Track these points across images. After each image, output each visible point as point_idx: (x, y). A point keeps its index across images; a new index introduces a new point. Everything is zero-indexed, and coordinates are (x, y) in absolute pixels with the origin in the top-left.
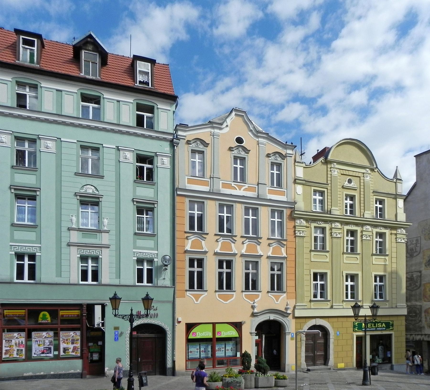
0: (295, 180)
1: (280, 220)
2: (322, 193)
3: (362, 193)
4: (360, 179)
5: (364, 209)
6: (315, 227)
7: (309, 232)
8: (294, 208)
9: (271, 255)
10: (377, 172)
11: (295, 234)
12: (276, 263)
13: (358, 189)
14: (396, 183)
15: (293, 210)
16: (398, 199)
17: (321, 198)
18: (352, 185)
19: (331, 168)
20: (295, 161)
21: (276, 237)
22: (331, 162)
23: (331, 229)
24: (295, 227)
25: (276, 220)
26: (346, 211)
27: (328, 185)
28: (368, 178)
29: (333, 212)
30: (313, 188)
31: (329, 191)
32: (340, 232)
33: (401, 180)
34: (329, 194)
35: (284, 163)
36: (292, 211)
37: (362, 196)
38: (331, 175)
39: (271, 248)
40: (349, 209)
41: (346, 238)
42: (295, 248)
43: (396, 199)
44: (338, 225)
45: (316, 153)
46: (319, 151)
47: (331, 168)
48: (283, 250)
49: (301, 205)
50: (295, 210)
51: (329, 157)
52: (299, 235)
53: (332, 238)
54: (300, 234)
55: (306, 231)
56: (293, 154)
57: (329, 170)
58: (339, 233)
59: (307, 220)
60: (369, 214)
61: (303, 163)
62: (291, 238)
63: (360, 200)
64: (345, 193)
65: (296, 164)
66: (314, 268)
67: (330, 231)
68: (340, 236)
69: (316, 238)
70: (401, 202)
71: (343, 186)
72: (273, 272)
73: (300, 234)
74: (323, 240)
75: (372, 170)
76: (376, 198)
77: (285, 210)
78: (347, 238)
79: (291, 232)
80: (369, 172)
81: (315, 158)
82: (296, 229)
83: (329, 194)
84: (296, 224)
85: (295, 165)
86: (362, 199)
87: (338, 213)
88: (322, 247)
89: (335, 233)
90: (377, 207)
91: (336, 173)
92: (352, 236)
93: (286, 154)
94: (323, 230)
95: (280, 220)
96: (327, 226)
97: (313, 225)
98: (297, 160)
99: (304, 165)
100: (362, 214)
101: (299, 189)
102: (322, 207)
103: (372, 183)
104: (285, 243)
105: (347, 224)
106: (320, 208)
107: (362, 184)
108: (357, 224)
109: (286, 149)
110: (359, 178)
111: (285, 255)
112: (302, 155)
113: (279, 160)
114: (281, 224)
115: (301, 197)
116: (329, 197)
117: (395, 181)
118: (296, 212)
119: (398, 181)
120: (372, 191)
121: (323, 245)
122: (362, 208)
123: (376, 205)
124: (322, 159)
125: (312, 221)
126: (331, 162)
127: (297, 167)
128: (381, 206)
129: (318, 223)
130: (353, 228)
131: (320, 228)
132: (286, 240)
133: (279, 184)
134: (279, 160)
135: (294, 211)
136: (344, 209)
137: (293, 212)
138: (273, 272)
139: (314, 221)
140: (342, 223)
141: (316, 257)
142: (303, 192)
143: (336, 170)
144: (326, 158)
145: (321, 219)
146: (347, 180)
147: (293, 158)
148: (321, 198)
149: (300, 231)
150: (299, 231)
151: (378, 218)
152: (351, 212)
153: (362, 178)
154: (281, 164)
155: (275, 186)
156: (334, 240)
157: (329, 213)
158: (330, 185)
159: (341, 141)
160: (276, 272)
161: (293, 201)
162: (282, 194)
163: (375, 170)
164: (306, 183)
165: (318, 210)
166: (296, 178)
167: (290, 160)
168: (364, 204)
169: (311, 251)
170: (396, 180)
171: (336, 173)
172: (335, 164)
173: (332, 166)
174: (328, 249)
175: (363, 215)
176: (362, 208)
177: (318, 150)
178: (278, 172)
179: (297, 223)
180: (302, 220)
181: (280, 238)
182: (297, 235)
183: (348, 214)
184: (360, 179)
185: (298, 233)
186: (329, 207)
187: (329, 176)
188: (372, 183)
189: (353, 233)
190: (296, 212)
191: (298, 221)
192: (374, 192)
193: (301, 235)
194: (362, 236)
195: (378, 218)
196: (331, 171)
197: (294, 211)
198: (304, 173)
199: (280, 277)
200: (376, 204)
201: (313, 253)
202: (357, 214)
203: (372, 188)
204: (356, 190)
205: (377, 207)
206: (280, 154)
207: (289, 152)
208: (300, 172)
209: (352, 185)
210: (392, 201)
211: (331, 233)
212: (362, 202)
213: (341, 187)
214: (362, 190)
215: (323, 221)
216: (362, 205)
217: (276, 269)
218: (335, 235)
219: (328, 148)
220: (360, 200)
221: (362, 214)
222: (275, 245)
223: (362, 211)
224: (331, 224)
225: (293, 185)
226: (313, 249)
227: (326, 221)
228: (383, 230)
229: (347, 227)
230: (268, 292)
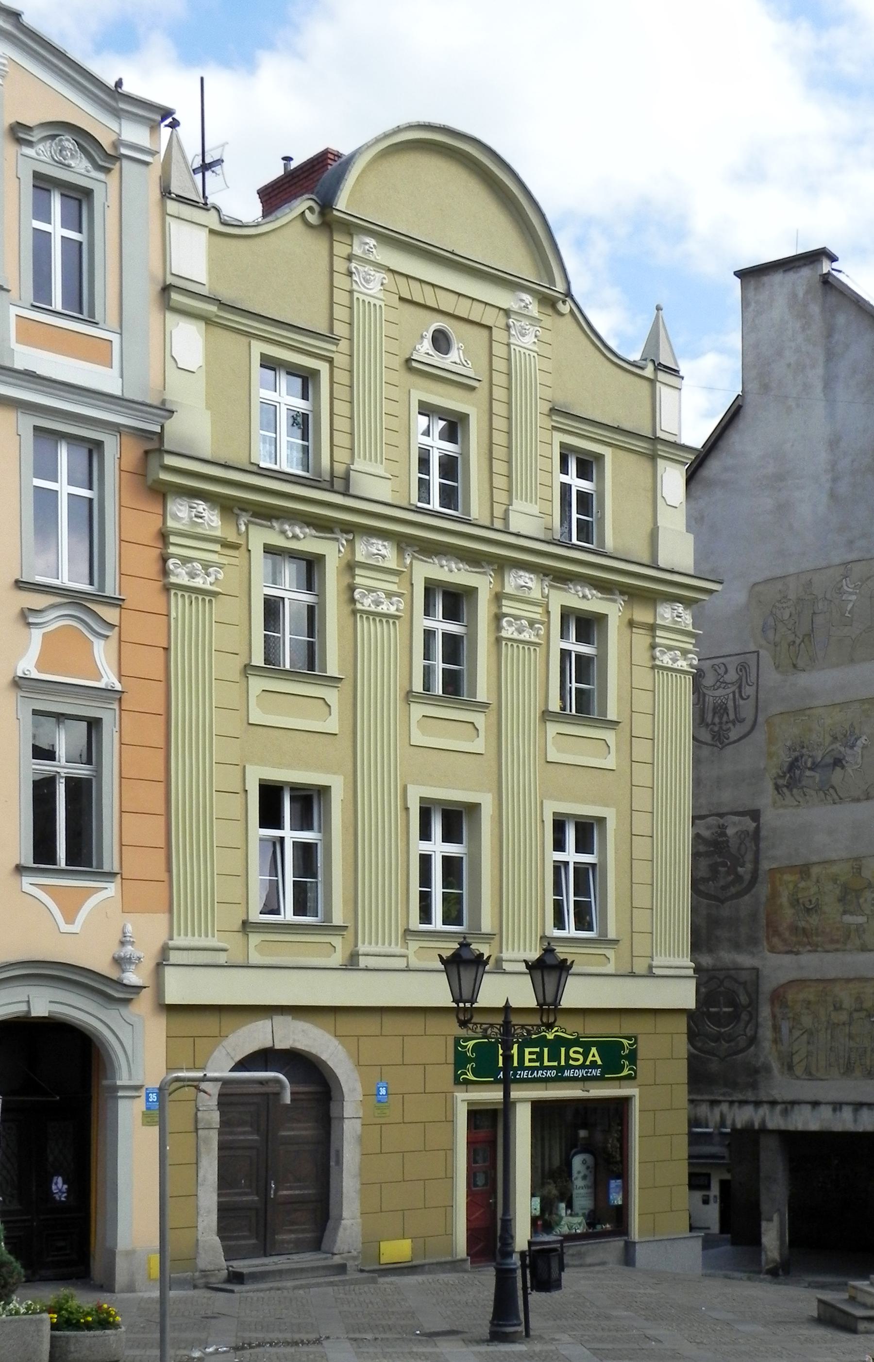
0: (166, 289)
1: (85, 493)
2: (307, 380)
3: (499, 408)
4: (491, 340)
5: (509, 491)
6: (270, 550)
7: (235, 575)
8: (161, 436)
9: (35, 674)
10: (569, 319)
11: (165, 572)
12: (60, 717)
13: (482, 388)
14: (652, 382)
15: (153, 445)
16: (661, 463)
17: (301, 405)
18: (453, 359)
19: (350, 258)
20: (166, 193)
21: (64, 580)
22: (351, 228)
23: (351, 567)
24: (164, 536)
25: (64, 488)
26: (424, 485)
27: (334, 340)
28: (528, 340)
29: (364, 485)
30: (258, 348)
31: (341, 377)
32: (394, 588)
33: (674, 372)
34: (341, 392)
35: (105, 190)
36: (147, 453)
37: (499, 423)
38: (351, 292)
39: (37, 635)
40: (435, 480)
41: (422, 623)
42: (167, 649)
43: (653, 457)
44: (384, 552)
45: (277, 171)
46: (294, 165)
47: (350, 258)
48: (102, 653)
49: (195, 427)
50: (166, 447)
51: (342, 202)
52: (184, 580)
53: (354, 612)
54: (192, 575)
55: (221, 566)
56: (153, 153)
57: (340, 265)
58: (389, 595)
59: (229, 508)
60: (532, 516)
61: (205, 207)
62: (143, 593)
63: (491, 443)
64: (417, 395)
65: (172, 207)
66: (262, 762)
67: (347, 580)
68: (392, 610)
69: (272, 609)
70: (673, 479)
71: (409, 360)
72: (46, 767)
73: (192, 575)
74: (313, 617)
75: (549, 302)
76: (563, 445)
77: (111, 444)
78: (430, 624)
79: (145, 560)
80: (534, 309)
81: (273, 196)
82: (172, 550)
83: (341, 392)
84: (171, 523)
85: (164, 213)
86: (499, 438)
87: (382, 491)
88: (304, 652)
89: (371, 590)
90: (566, 489)
91: (372, 287)
92: (452, 613)
93: (116, 145)
94: (311, 568)
95: (85, 493)
96: (332, 552)
97: (260, 536)
98: (175, 189)
99: (211, 219)
100: (498, 511)
101: (188, 341)
102: (305, 450)
103: (546, 365)
104: (110, 614)
105: (430, 550)
106: (298, 455)
107: (499, 364)
108: (474, 559)
109: (117, 114)
110: (485, 333)
111: (109, 679)
112: (205, 167)
113: (79, 169)
114: (89, 516)
115: (199, 383)
116: (341, 408)
117: (649, 372)
118: (170, 460)
119: (662, 376)
120: (545, 407)
121: (311, 646)
122: (500, 482)
123: (564, 479)
124: (302, 204)
125: (256, 515)
126: (351, 228)
127: (174, 226)
128: (585, 485)
129: (283, 532)
130: (457, 574)
131: (294, 555)
132: (116, 603)
133: (79, 302)
134: (79, 169)
135: (161, 451)
136: (415, 475)
137: (153, 461)
138: (46, 767)
139: (266, 515)
140: (402, 542)
141: (277, 706)
142: (207, 363)
143: (379, 276)
144: (326, 205)
145: (303, 512)
146: (429, 335)
147: (155, 171)
148: (301, 405)
149: (190, 560)
150: (186, 560)
151: (574, 540)
152: (449, 496)
153: (498, 334)
154: (88, 193)
155: (57, 303)
156: (364, 626)
157: (338, 484)
158: (344, 345)
159: (398, 130)
160: (63, 767)
161: (156, 402)
162: (99, 352)
163: (560, 306)
164: (222, 314)
165: (288, 461)
166: (170, 280)
167: (140, 185)
168: (509, 462)
169: (248, 669)
170: (656, 369)
171: (375, 288)
172: (372, 242)
173: (357, 251)
174: (332, 670)
175: (506, 519)
176: (500, 482)
177: (287, 159)
178: (73, 235)
179: (176, 518)
180: (201, 506)
181: (85, 587)
182: (173, 579)
183: (435, 504)
184: (491, 340)
185: (182, 571)
186: (341, 455)
187: (340, 297)
188: (546, 365)
189: (455, 601)
190: (170, 460)
191: (180, 512)
192: (553, 411)
193: (198, 582)
194: (498, 618)
195: (574, 540)
196: (350, 274)
197: (161, 451)
198: (214, 262)
199: (81, 793)
200: (564, 470)
201: (257, 684)
202: (477, 510)
203: (548, 394)
204: (472, 389)
205: (566, 489)
206: (85, 140)
207: (134, 133)
208: (191, 255)
209: (453, 359)
210: (636, 467)
211: (352, 588)
212: (499, 452)
213: (397, 362)
214: (499, 393)
215: (308, 525)
216: (499, 467)
217: (61, 751)
218: (367, 603)
219: (338, 155)
220: (491, 443)
221: (498, 511)
222: (55, 621)
223: (500, 496)
224: (351, 542)
225: (154, 316)
226: (258, 660)
227: (323, 526)
228: (592, 602)
229: (426, 569)
230: (20, 869)
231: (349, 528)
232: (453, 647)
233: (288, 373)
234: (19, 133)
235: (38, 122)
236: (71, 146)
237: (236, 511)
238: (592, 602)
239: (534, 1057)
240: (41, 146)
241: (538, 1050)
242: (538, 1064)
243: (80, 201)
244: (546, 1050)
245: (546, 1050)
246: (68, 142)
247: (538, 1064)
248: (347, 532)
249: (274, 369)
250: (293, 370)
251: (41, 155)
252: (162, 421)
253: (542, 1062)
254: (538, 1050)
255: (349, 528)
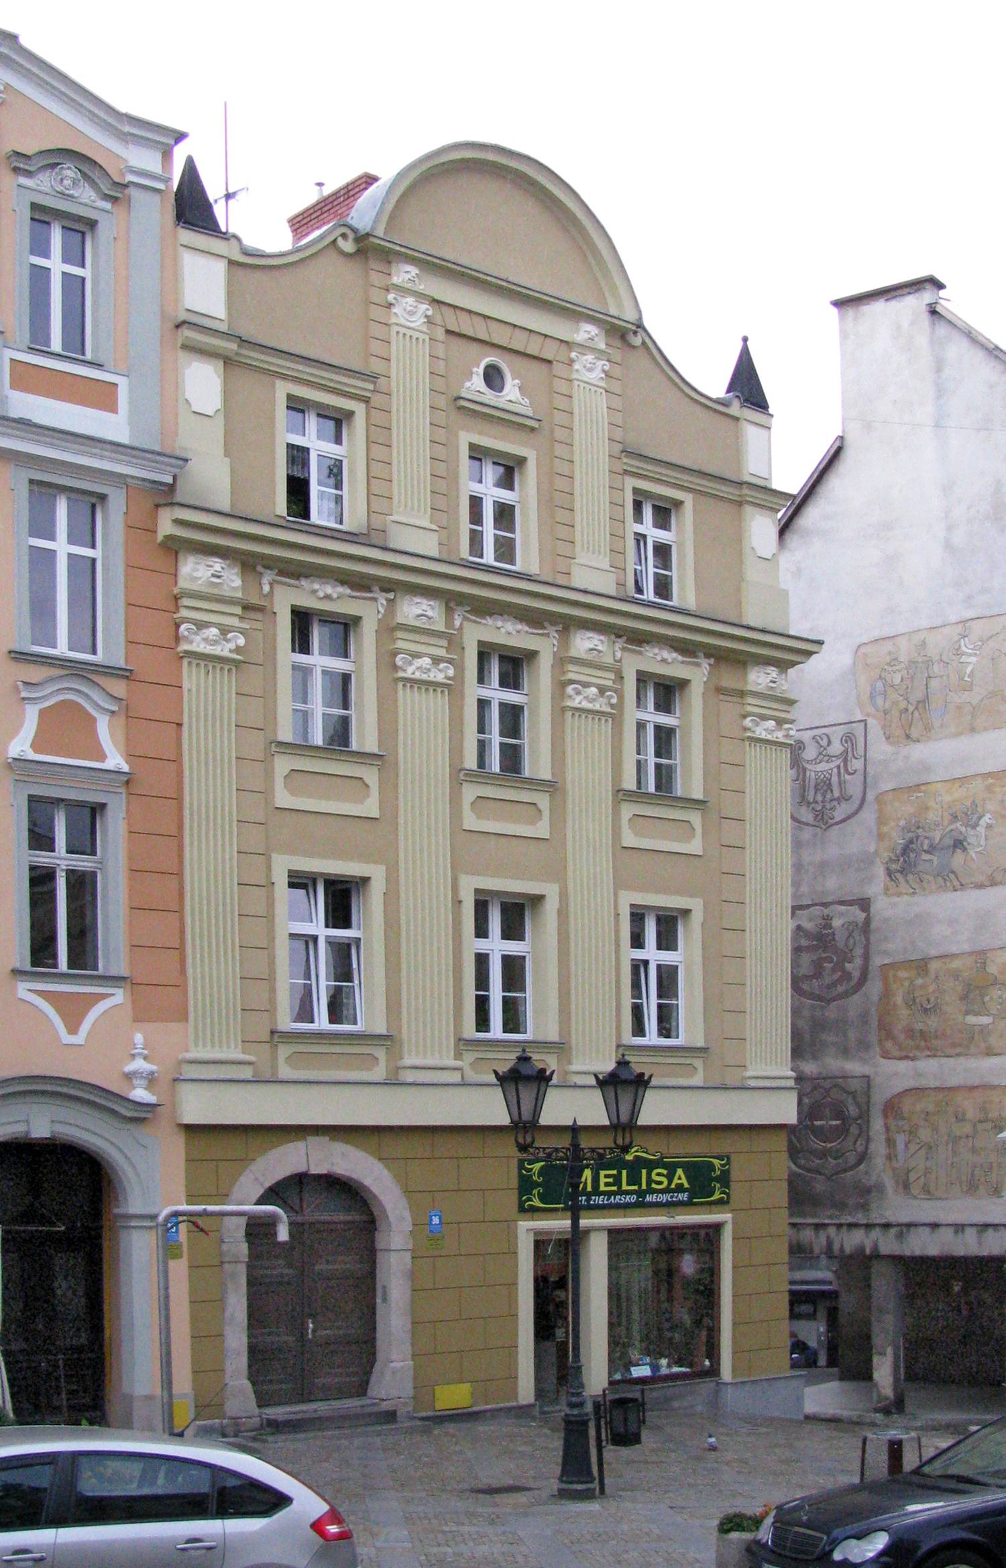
30: (282, 389)
41: (473, 691)
68: (440, 677)
105: (483, 609)
108: (534, 619)
113: (86, 200)
115: (217, 429)
125: (281, 573)
136: (465, 526)
140: (451, 601)
183: (489, 557)
194: (561, 686)
205: (640, 538)
215: (343, 583)
227: (360, 584)
229: (477, 632)
231: (388, 586)
232: (512, 717)
233: (319, 415)
234: (20, 163)
235: (37, 150)
236: (73, 175)
237: (260, 568)
238: (662, 661)
239: (611, 1180)
240: (40, 176)
241: (615, 1172)
242: (614, 1188)
243: (83, 234)
244: (624, 1173)
245: (624, 1173)
246: (70, 172)
247: (614, 1188)
248: (388, 591)
249: (303, 411)
250: (324, 413)
251: (43, 186)
252: (177, 471)
253: (620, 1186)
254: (615, 1172)
255: (388, 586)
